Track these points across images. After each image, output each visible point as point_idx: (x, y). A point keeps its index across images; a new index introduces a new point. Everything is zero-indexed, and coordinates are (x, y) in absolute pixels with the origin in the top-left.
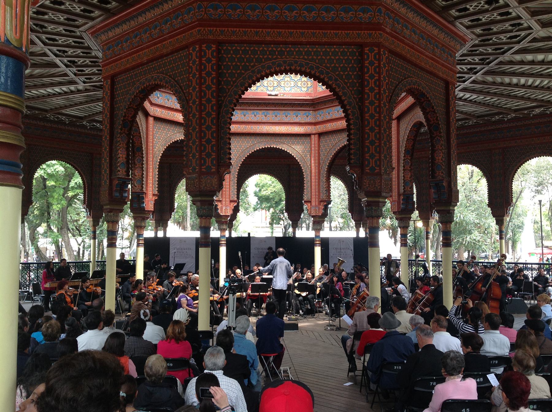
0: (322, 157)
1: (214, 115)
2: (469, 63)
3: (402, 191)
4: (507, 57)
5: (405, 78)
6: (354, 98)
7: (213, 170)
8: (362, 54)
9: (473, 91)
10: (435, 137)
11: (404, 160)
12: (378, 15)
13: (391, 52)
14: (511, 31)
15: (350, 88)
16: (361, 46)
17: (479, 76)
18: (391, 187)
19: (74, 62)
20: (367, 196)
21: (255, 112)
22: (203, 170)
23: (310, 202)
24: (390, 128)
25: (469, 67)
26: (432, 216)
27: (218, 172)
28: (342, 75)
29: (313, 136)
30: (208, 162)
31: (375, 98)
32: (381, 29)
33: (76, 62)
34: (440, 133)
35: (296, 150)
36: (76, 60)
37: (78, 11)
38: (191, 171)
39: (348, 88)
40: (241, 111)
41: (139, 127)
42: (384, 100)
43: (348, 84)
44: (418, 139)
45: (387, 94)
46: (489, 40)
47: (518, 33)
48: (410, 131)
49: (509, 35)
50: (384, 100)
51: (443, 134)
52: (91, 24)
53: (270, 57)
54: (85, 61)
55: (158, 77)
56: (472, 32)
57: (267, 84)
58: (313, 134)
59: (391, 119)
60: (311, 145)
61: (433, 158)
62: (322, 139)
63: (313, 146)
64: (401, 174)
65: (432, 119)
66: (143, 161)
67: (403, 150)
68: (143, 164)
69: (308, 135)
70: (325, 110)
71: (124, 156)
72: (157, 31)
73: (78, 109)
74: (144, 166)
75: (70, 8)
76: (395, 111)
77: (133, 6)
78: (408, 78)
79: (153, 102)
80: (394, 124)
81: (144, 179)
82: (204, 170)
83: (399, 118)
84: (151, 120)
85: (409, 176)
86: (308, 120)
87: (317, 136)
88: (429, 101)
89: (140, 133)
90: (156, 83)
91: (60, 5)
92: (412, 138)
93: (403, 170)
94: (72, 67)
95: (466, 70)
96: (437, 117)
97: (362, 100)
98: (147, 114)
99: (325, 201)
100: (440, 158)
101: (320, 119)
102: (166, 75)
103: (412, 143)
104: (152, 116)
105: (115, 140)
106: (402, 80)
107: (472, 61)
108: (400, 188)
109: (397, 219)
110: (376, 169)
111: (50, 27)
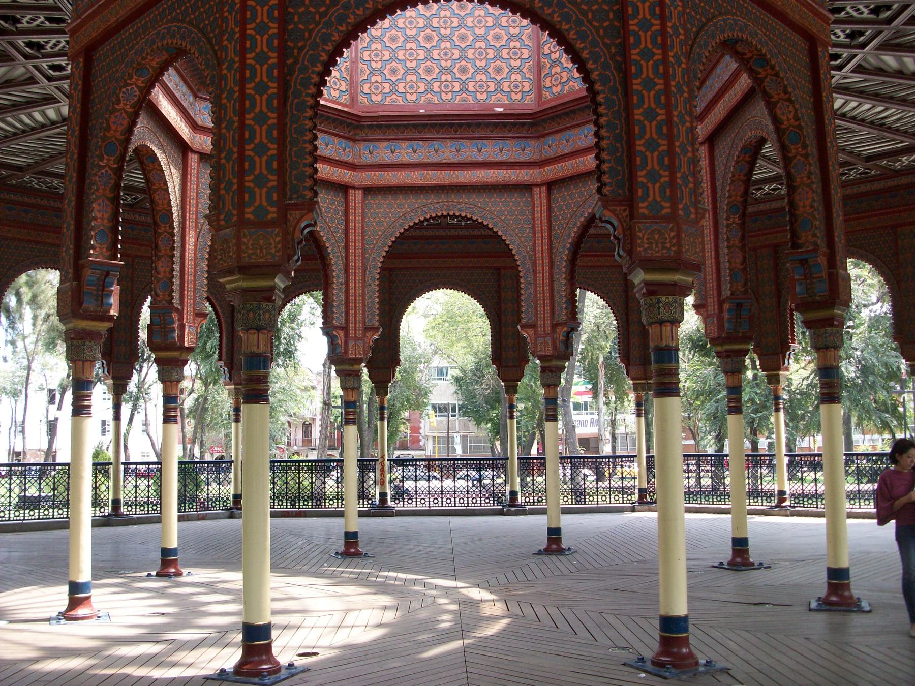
2: (850, 21)
3: (727, 293)
5: (721, 14)
6: (604, 44)
7: (269, 217)
10: (795, 156)
11: (728, 226)
15: (595, 24)
19: (39, 47)
20: (647, 270)
21: (414, 143)
22: (247, 216)
23: (533, 326)
24: (695, 161)
25: (849, 28)
26: (784, 363)
27: (282, 219)
29: (536, 190)
30: (261, 197)
31: (654, 43)
34: (805, 147)
35: (501, 216)
36: (41, 39)
38: (222, 223)
39: (590, 22)
40: (386, 144)
41: (162, 171)
42: (677, 49)
43: (590, 15)
44: (750, 209)
45: (684, 66)
48: (737, 162)
50: (677, 49)
51: (813, 150)
54: (59, 42)
57: (404, 23)
58: (537, 185)
60: (533, 208)
62: (556, 194)
63: (537, 209)
66: (174, 242)
67: (723, 205)
68: (173, 249)
70: (557, 136)
73: (39, 139)
74: (177, 253)
78: (726, 14)
79: (199, 123)
81: (176, 281)
82: (250, 217)
83: (712, 140)
84: (193, 159)
85: (739, 260)
86: (524, 158)
87: (544, 188)
88: (777, 75)
89: (165, 183)
90: (165, 42)
92: (742, 178)
93: (729, 247)
95: (842, 36)
96: (796, 111)
97: (624, 50)
99: (564, 324)
100: (808, 203)
101: (550, 154)
102: (182, 21)
103: (742, 189)
107: (855, 14)
108: (723, 287)
109: (719, 355)
110: (663, 208)
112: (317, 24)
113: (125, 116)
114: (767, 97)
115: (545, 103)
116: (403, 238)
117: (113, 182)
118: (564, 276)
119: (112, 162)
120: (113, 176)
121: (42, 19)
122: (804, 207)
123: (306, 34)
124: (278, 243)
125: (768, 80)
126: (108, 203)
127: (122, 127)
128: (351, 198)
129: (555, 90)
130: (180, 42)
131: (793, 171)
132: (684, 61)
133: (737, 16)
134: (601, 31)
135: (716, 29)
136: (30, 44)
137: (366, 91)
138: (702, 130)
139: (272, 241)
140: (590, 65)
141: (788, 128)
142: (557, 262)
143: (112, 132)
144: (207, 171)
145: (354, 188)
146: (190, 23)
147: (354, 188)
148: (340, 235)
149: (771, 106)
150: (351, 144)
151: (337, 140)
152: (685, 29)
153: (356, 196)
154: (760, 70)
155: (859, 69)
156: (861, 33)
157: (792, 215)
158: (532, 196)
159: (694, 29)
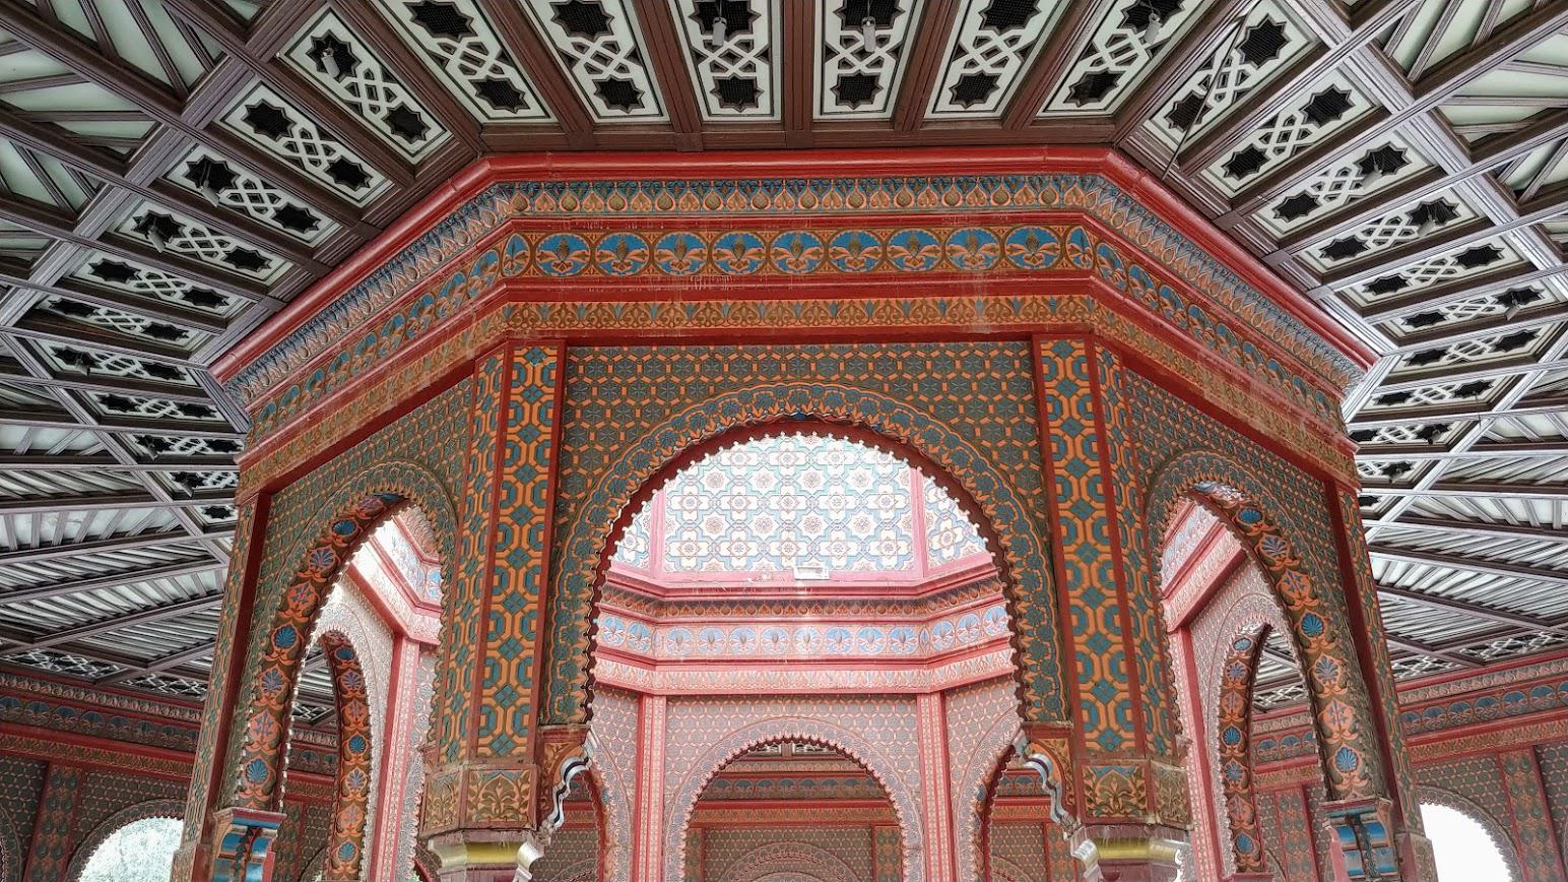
0: (957, 766)
1: (537, 558)
4: (1503, 421)
8: (1033, 363)
9: (1408, 551)
11: (1223, 761)
12: (1073, 250)
13: (1132, 361)
14: (1501, 320)
16: (1028, 337)
17: (1421, 496)
18: (1187, 806)
19: (193, 481)
25: (1389, 459)
28: (973, 428)
29: (923, 701)
32: (1084, 288)
33: (200, 482)
37: (177, 298)
41: (360, 672)
43: (995, 455)
46: (1436, 355)
47: (1527, 325)
49: (1499, 333)
52: (222, 340)
53: (734, 379)
55: (387, 470)
56: (1381, 328)
59: (1161, 635)
60: (920, 728)
61: (1319, 725)
64: (1222, 813)
65: (1294, 595)
66: (369, 780)
67: (1213, 725)
69: (912, 697)
71: (270, 739)
72: (396, 337)
74: (372, 798)
75: (153, 289)
76: (1168, 553)
77: (334, 268)
80: (1176, 645)
81: (367, 842)
83: (1187, 626)
87: (936, 699)
91: (123, 280)
94: (186, 497)
97: (1049, 505)
98: (397, 635)
100: (1347, 725)
103: (1240, 703)
104: (416, 642)
105: (243, 688)
106: (1177, 452)
111: (108, 358)
112: (606, 468)
113: (312, 589)
114: (1264, 564)
115: (934, 571)
116: (720, 776)
117: (283, 687)
118: (971, 838)
119: (284, 657)
120: (285, 678)
121: (203, 444)
122: (1341, 731)
123: (590, 481)
124: (526, 792)
125: (1263, 540)
126: (272, 719)
127: (307, 605)
128: (648, 711)
129: (946, 554)
130: (401, 489)
131: (1316, 675)
132: (1138, 518)
133: (1208, 448)
134: (1012, 477)
135: (1182, 469)
136: (179, 478)
137: (675, 552)
138: (1174, 610)
139: (515, 789)
140: (998, 526)
141: (1301, 611)
142: (958, 816)
143: (289, 612)
144: (430, 673)
145: (652, 696)
146: (420, 462)
147: (652, 696)
148: (628, 768)
149: (1272, 579)
150: (649, 629)
151: (629, 623)
152: (1136, 472)
153: (655, 708)
154: (1251, 526)
155: (1408, 517)
156: (1406, 467)
157: (1323, 745)
158: (918, 712)
159: (1149, 471)
